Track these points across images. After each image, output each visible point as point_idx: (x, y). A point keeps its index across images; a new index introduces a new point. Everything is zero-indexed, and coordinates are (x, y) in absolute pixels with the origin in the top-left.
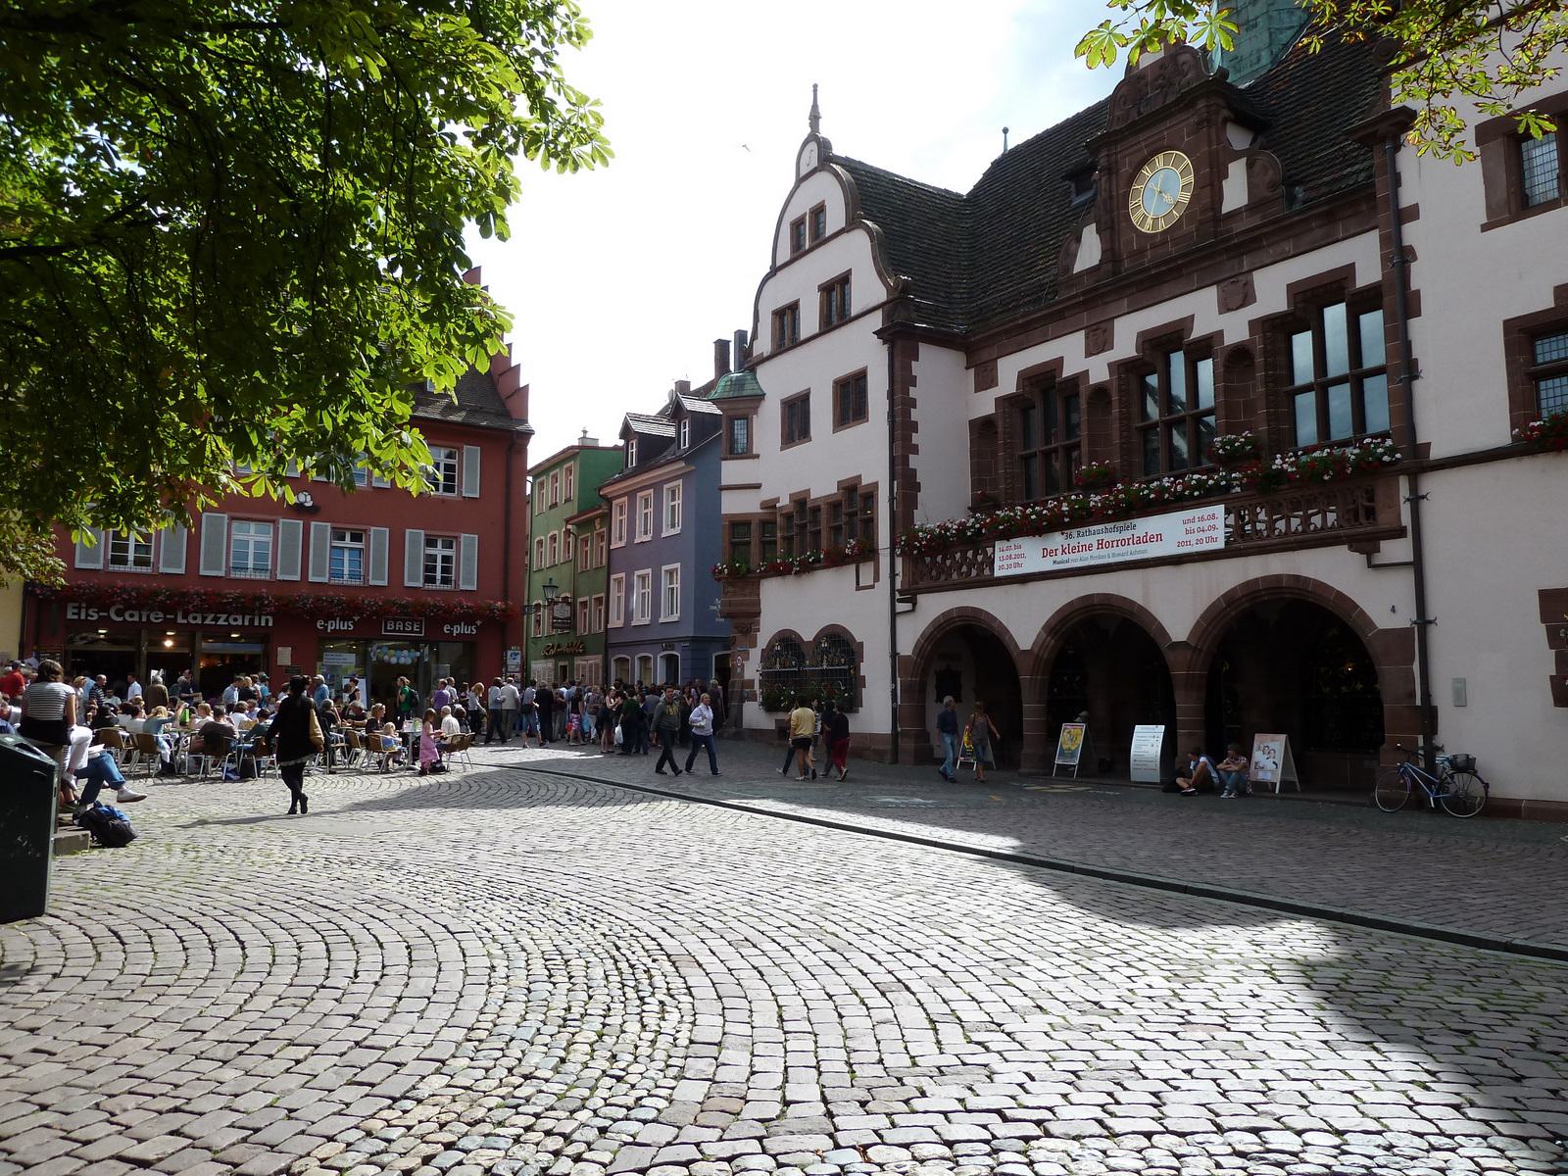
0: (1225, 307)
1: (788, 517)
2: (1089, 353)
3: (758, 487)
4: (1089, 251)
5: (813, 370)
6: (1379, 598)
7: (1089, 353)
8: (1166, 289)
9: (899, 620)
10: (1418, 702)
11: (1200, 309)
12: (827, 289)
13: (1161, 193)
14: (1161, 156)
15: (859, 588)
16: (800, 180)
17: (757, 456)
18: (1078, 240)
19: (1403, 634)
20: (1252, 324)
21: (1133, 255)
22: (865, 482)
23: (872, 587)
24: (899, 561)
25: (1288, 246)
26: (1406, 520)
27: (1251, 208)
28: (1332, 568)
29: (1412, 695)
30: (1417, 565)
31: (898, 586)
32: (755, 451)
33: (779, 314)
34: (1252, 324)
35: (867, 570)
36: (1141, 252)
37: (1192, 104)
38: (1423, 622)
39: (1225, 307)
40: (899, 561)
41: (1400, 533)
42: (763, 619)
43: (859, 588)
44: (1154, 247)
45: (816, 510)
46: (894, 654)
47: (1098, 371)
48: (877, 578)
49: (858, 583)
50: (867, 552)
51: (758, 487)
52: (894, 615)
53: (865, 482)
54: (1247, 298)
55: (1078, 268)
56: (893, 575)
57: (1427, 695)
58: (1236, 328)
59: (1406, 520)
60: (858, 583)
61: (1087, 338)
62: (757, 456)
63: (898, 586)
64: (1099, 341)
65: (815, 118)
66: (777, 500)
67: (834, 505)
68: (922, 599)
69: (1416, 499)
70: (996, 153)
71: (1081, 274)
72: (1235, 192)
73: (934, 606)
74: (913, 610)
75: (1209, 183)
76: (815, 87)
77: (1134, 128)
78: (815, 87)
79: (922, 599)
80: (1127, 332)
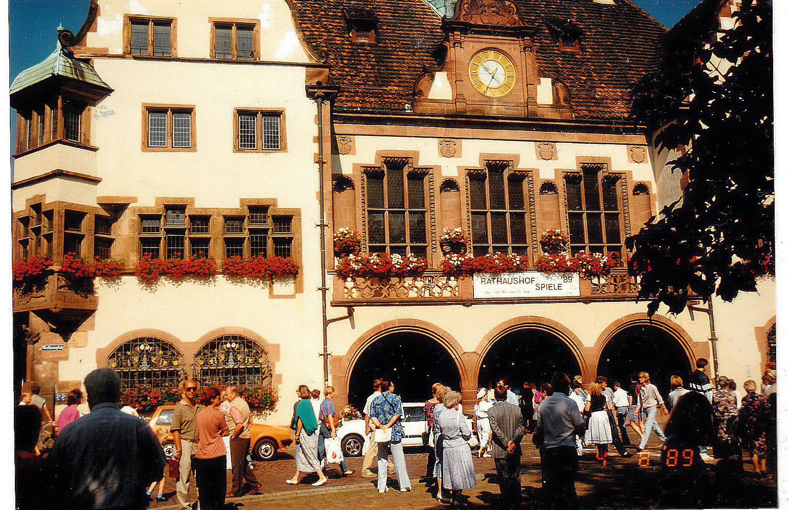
3: (95, 181)
4: (440, 88)
5: (216, 94)
14: (492, 52)
17: (95, 149)
23: (293, 296)
32: (93, 143)
38: (713, 339)
39: (542, 157)
42: (99, 317)
45: (202, 220)
46: (325, 355)
48: (299, 289)
49: (271, 292)
51: (95, 181)
52: (326, 323)
58: (547, 171)
66: (134, 200)
67: (233, 220)
68: (357, 310)
79: (357, 310)
80: (475, 150)
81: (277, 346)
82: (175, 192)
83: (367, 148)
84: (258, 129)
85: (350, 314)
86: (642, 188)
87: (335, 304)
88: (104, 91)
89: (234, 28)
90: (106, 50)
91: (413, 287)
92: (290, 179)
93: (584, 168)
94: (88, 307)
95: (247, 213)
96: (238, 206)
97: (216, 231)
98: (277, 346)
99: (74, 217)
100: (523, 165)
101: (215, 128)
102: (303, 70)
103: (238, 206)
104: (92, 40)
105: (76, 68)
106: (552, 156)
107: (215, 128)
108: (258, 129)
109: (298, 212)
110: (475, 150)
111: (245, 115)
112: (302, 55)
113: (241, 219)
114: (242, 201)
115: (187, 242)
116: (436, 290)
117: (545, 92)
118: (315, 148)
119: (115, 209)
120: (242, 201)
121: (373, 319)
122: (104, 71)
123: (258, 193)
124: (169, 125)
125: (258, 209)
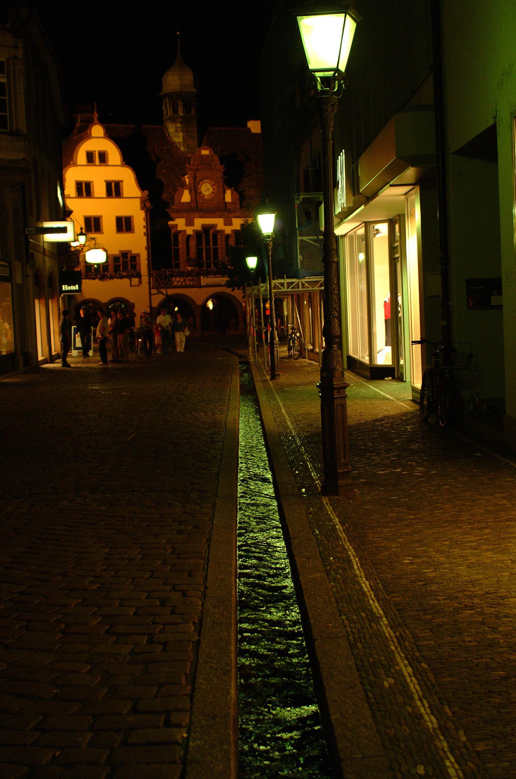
0: (226, 224)
4: (186, 197)
9: (152, 296)
11: (219, 223)
20: (232, 231)
22: (133, 252)
23: (139, 286)
34: (232, 231)
35: (135, 281)
39: (226, 224)
40: (151, 279)
43: (131, 286)
47: (190, 231)
48: (140, 282)
49: (131, 284)
50: (139, 276)
52: (150, 295)
54: (231, 224)
56: (150, 283)
60: (131, 284)
61: (186, 220)
80: (199, 223)
87: (153, 288)
90: (69, 195)
91: (177, 281)
96: (118, 253)
100: (219, 228)
103: (118, 253)
106: (231, 224)
109: (139, 255)
111: (119, 220)
113: (120, 257)
114: (120, 251)
116: (188, 282)
120: (120, 251)
123: (125, 248)
125: (125, 254)
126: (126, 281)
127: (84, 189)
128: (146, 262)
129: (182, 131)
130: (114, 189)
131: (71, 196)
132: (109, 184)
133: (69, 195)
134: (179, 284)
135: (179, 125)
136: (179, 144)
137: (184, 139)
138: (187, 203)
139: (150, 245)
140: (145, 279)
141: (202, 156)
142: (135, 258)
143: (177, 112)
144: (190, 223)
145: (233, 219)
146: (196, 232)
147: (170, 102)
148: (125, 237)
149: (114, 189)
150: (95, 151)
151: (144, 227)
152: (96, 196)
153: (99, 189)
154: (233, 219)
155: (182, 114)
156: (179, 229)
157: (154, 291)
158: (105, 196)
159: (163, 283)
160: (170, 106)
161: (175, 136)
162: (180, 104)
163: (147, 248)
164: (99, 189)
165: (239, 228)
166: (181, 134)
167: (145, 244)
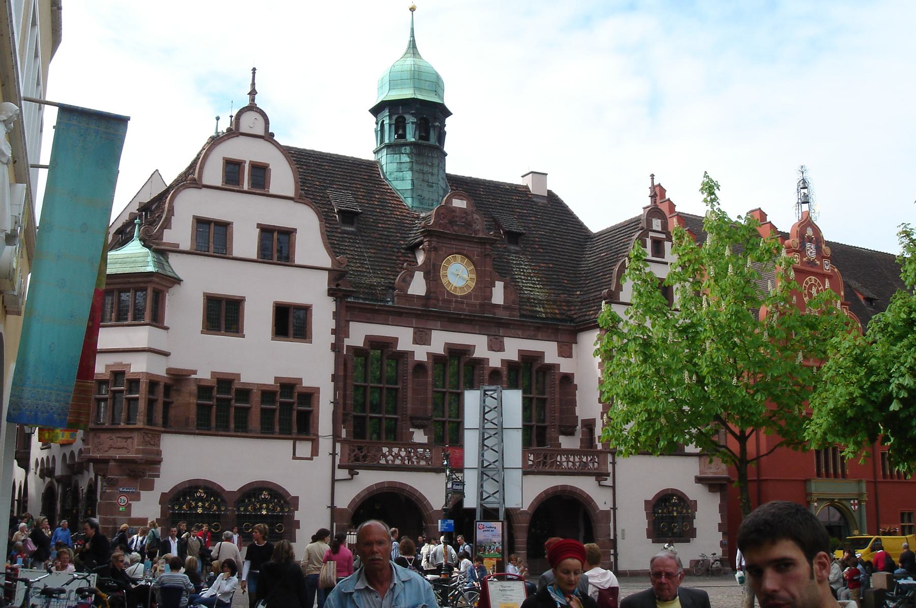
0: (491, 348)
1: (204, 390)
2: (416, 342)
3: (166, 354)
4: (418, 286)
6: (601, 499)
7: (416, 342)
8: (462, 326)
9: (337, 485)
10: (612, 537)
12: (266, 231)
13: (458, 275)
15: (295, 458)
16: (234, 132)
17: (167, 328)
18: (412, 276)
19: (608, 512)
21: (444, 300)
22: (306, 383)
23: (311, 459)
24: (338, 446)
25: (520, 333)
26: (610, 469)
27: (504, 307)
28: (586, 485)
29: (609, 535)
30: (613, 487)
31: (337, 462)
32: (166, 324)
33: (201, 223)
35: (304, 448)
36: (450, 301)
37: (485, 243)
38: (614, 508)
39: (491, 348)
40: (338, 446)
41: (608, 475)
42: (164, 468)
43: (295, 458)
44: (456, 302)
45: (245, 393)
46: (332, 507)
48: (315, 452)
51: (166, 354)
52: (334, 481)
53: (304, 384)
54: (501, 349)
55: (410, 292)
56: (334, 454)
57: (615, 535)
58: (495, 360)
59: (610, 469)
61: (415, 333)
62: (167, 328)
63: (337, 462)
64: (422, 338)
65: (253, 93)
66: (195, 372)
67: (267, 394)
69: (614, 463)
70: (213, 134)
71: (413, 296)
72: (498, 295)
73: (369, 479)
74: (352, 479)
75: (484, 286)
76: (254, 69)
77: (457, 238)
78: (254, 69)
80: (441, 340)
81: (297, 498)
82: (226, 367)
83: (359, 333)
84: (290, 322)
85: (353, 473)
86: (567, 379)
87: (340, 467)
88: (178, 281)
89: (276, 234)
90: (178, 245)
91: (391, 453)
92: (312, 364)
93: (522, 359)
94: (157, 458)
95: (278, 389)
96: (272, 382)
97: (256, 405)
98: (297, 498)
99: (153, 383)
101: (258, 318)
102: (327, 272)
103: (272, 382)
104: (169, 237)
105: (158, 263)
106: (501, 349)
107: (258, 318)
108: (290, 322)
110: (441, 340)
112: (327, 262)
115: (233, 410)
117: (498, 295)
118: (332, 339)
119: (178, 378)
121: (369, 479)
122: (178, 265)
123: (289, 373)
124: (223, 315)
125: (288, 386)
126: (283, 447)
127: (213, 237)
128: (331, 407)
129: (411, 169)
130: (276, 246)
131: (181, 248)
132: (266, 231)
133: (178, 245)
134: (398, 462)
135: (405, 159)
136: (403, 194)
137: (413, 184)
138: (419, 297)
139: (341, 373)
140: (325, 445)
141: (454, 210)
142: (309, 396)
143: (403, 136)
144: (422, 338)
145: (506, 340)
146: (436, 358)
147: (390, 117)
148: (291, 347)
149: (276, 246)
150: (245, 162)
151: (334, 332)
152: (236, 254)
153: (245, 242)
154: (506, 340)
155: (413, 140)
156: (400, 347)
157: (342, 474)
158: (255, 257)
159: (365, 457)
160: (390, 125)
161: (397, 179)
162: (410, 119)
163: (334, 378)
164: (245, 242)
165: (515, 357)
166: (408, 175)
167: (331, 370)
